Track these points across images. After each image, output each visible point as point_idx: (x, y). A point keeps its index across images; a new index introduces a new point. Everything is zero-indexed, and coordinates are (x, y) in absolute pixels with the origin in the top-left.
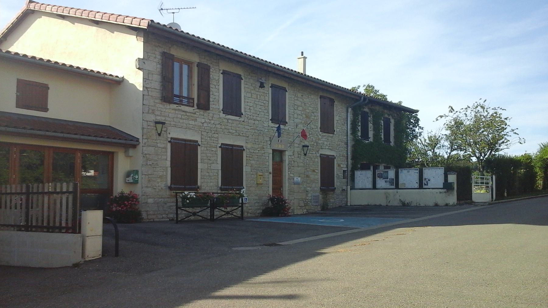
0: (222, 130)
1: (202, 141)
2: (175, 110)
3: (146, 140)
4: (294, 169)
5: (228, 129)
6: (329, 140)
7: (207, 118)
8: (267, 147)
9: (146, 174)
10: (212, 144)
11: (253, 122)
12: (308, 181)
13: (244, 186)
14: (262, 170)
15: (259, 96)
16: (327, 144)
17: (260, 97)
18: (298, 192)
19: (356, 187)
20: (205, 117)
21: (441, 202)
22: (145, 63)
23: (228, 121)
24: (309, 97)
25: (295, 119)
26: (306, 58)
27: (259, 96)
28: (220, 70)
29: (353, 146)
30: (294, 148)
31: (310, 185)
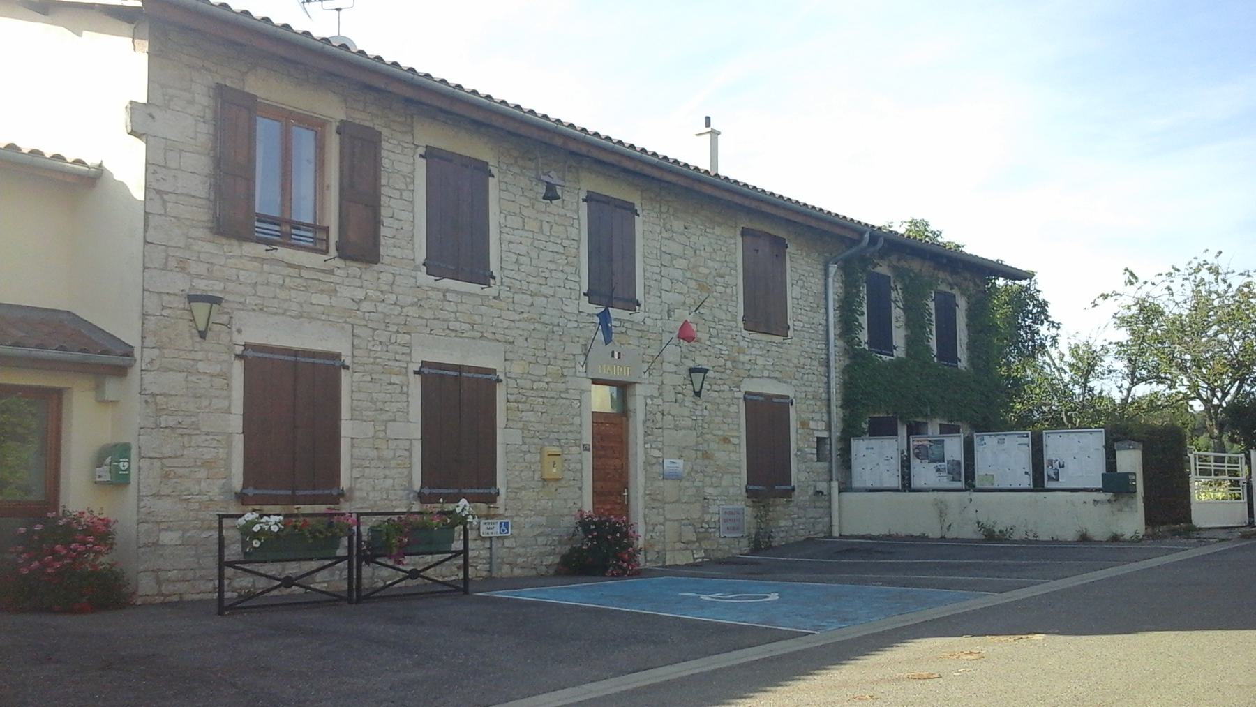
0: (424, 322)
1: (353, 356)
2: (263, 260)
3: (156, 351)
4: (663, 436)
5: (444, 320)
6: (770, 353)
7: (371, 287)
9: (152, 455)
10: (390, 363)
11: (530, 299)
12: (709, 470)
13: (498, 486)
14: (559, 440)
15: (546, 227)
16: (765, 365)
17: (551, 229)
18: (678, 501)
19: (856, 484)
20: (365, 284)
21: (1098, 530)
22: (152, 117)
23: (444, 296)
24: (707, 230)
25: (663, 292)
26: (718, 133)
27: (546, 227)
28: (417, 146)
29: (846, 370)
30: (661, 376)
31: (714, 480)
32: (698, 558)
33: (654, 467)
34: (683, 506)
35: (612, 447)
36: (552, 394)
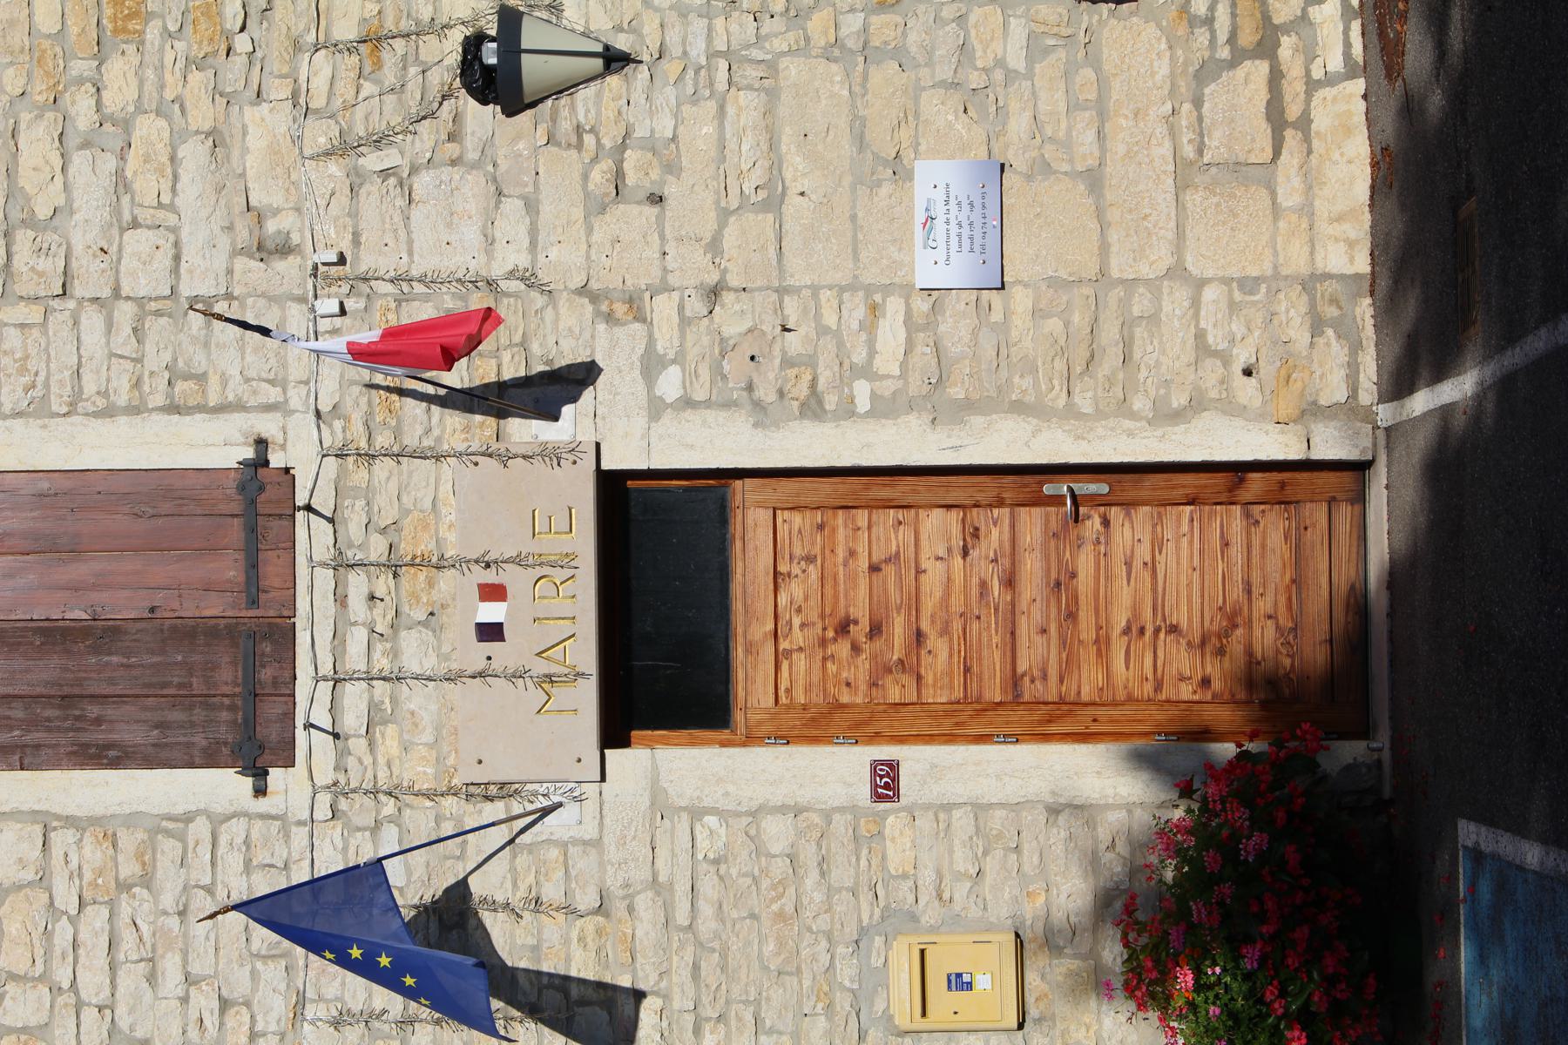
4: (815, 290)
8: (585, 843)
14: (863, 931)
18: (1094, 179)
32: (1347, 45)
33: (954, 349)
34: (1118, 148)
35: (874, 569)
36: (682, 975)
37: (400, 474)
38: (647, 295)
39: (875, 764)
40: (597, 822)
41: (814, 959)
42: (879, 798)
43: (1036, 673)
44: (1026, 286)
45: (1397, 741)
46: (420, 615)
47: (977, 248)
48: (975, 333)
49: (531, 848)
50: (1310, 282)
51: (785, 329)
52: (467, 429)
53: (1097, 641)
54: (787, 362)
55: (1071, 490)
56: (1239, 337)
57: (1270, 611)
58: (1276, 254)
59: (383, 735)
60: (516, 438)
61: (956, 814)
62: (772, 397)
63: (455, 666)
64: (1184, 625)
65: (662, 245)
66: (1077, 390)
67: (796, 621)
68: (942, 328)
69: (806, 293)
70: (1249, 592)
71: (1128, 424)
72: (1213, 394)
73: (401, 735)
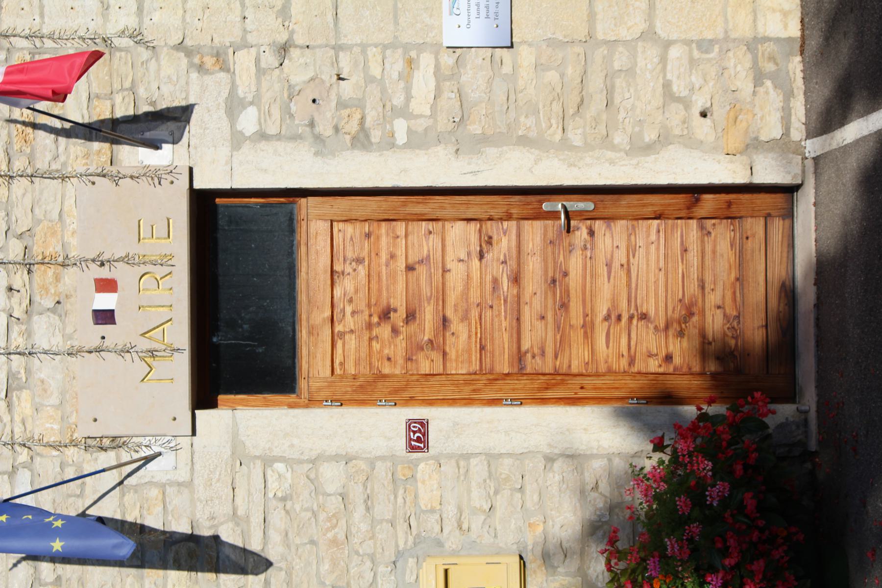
4: (364, 47)
8: (180, 484)
14: (399, 554)
33: (473, 94)
35: (410, 268)
37: (33, 191)
38: (231, 51)
39: (409, 423)
40: (189, 467)
41: (361, 576)
42: (413, 449)
43: (536, 350)
44: (530, 45)
45: (823, 404)
46: (49, 303)
47: (492, 15)
48: (490, 82)
49: (136, 488)
50: (753, 44)
51: (340, 79)
52: (87, 156)
53: (584, 326)
54: (341, 104)
55: (564, 207)
56: (697, 86)
57: (719, 303)
58: (726, 21)
59: (19, 398)
60: (126, 163)
61: (474, 461)
62: (329, 132)
63: (76, 344)
64: (652, 313)
65: (243, 11)
66: (570, 127)
67: (349, 309)
68: (464, 79)
69: (357, 50)
70: (703, 288)
71: (610, 154)
72: (677, 131)
73: (33, 399)
